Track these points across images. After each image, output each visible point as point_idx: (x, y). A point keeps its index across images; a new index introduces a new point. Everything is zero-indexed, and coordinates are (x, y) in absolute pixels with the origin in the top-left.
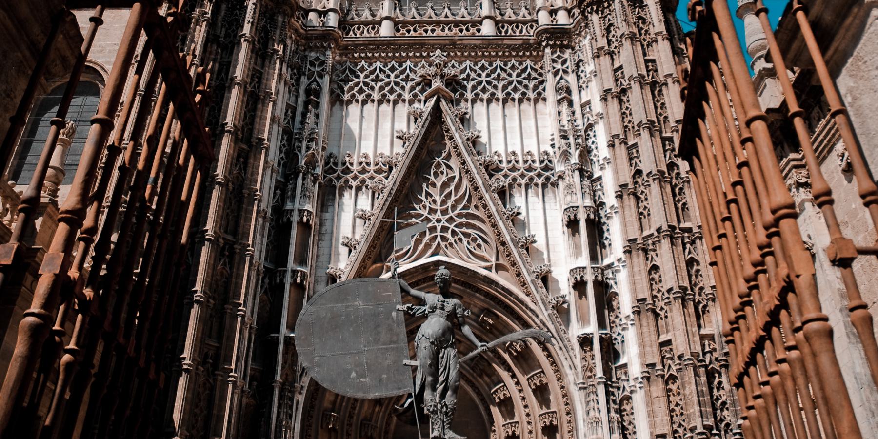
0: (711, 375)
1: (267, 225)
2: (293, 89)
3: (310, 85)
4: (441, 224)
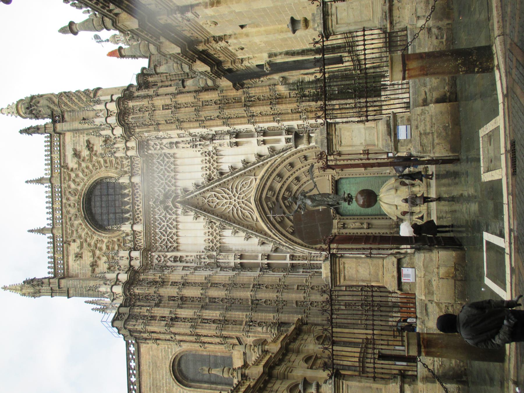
0: (305, 96)
1: (242, 273)
2: (173, 269)
3: (171, 261)
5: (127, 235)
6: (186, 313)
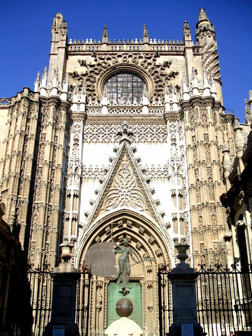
3: (75, 137)
5: (99, 102)
6: (30, 147)
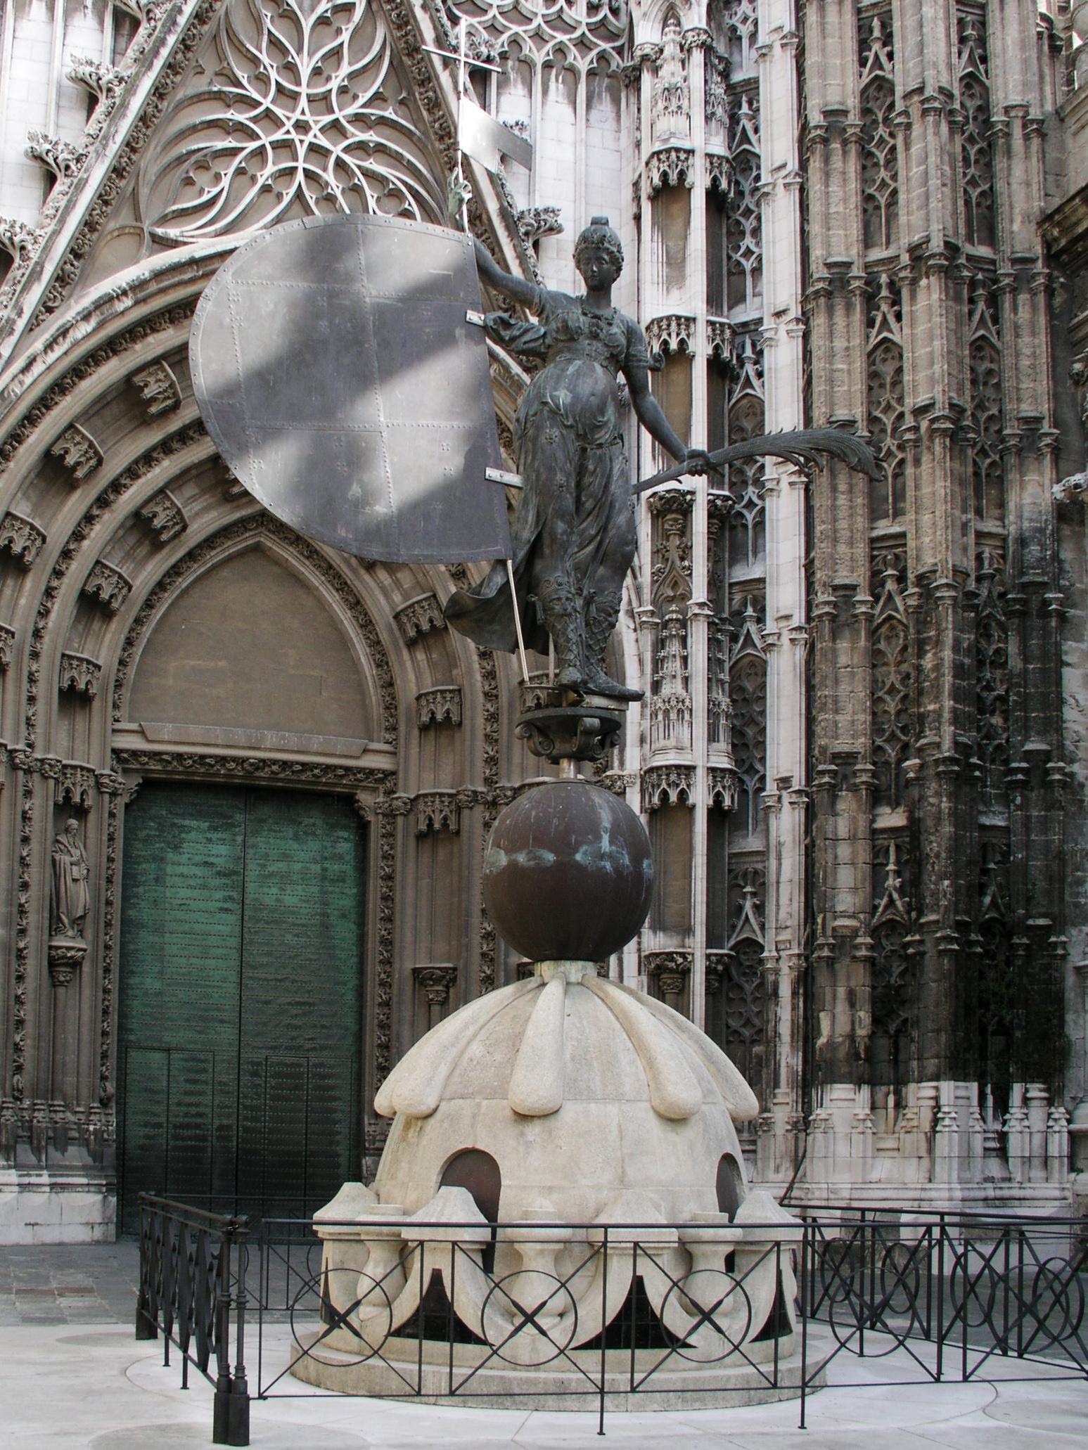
4: (309, 138)
